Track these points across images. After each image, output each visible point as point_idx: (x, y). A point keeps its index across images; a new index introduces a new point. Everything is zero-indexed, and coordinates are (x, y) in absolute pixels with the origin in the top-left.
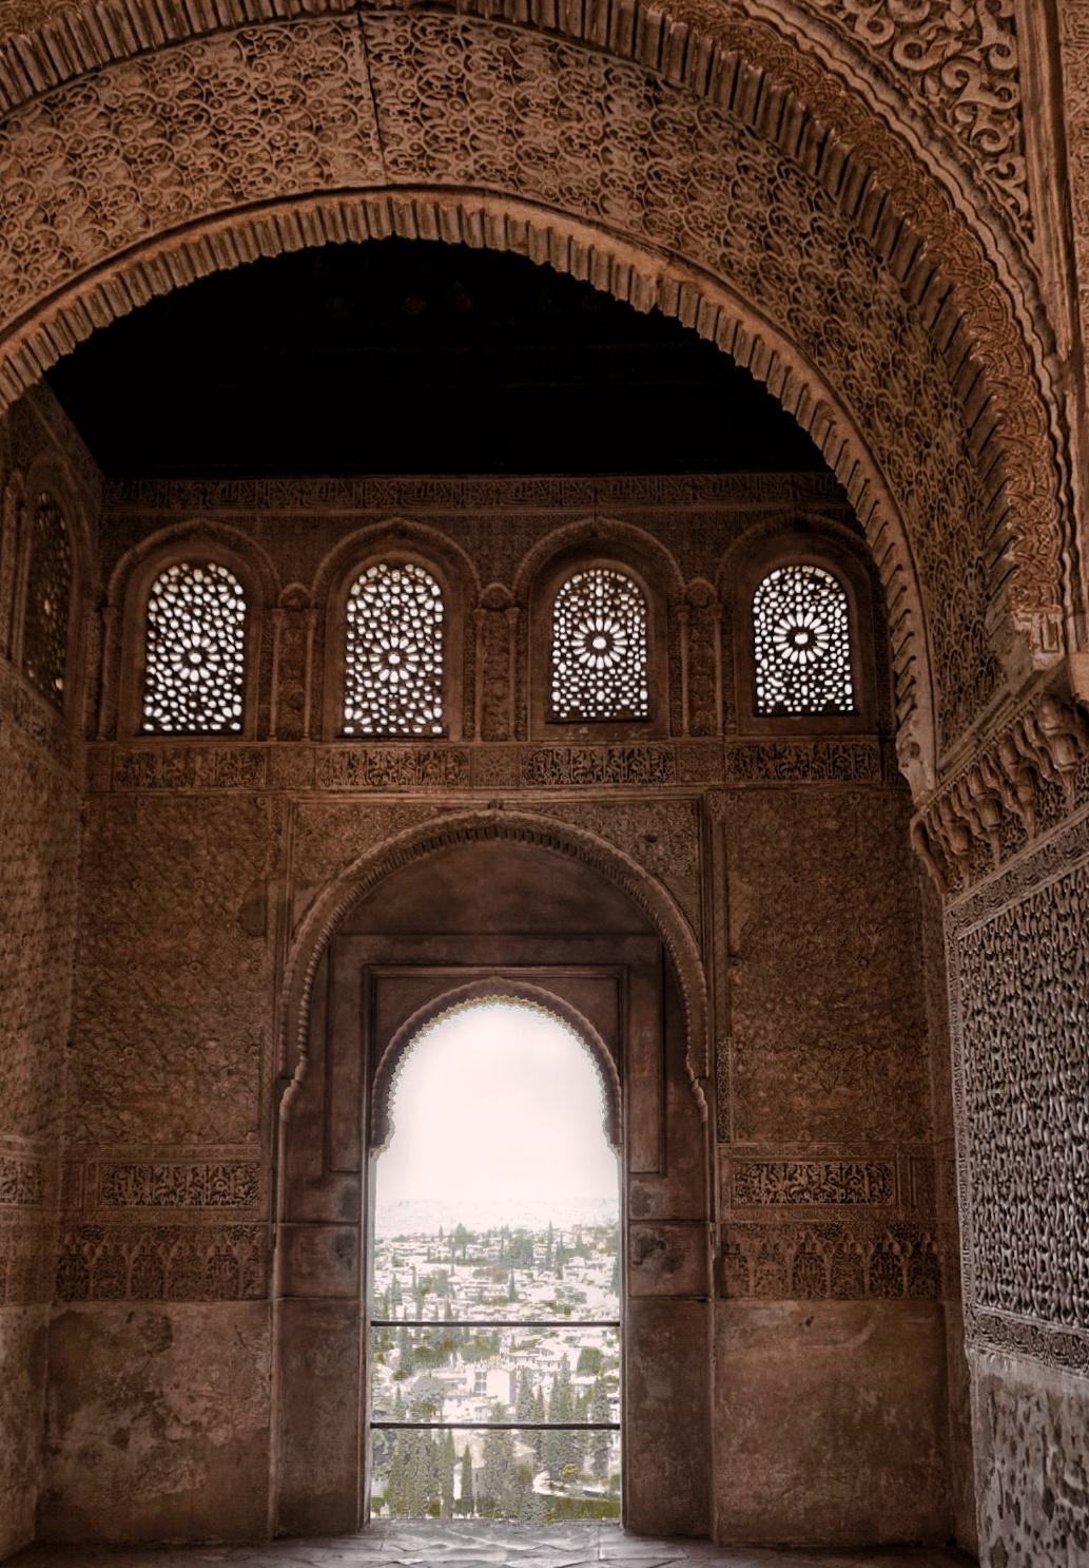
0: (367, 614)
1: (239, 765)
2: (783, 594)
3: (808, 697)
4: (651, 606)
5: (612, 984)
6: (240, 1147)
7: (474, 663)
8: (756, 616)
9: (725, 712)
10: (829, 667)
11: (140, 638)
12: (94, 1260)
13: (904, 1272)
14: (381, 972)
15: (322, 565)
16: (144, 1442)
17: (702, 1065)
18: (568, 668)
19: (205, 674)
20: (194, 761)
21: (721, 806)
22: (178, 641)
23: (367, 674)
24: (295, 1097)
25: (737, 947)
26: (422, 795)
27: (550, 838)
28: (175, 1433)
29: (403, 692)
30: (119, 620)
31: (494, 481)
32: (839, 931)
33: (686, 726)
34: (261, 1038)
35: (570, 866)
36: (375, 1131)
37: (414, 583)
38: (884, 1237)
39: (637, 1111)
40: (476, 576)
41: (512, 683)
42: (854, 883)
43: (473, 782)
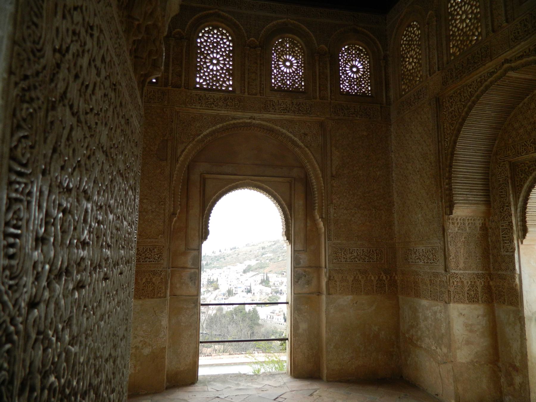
2: (349, 54)
3: (356, 89)
6: (156, 240)
9: (331, 93)
10: (363, 80)
14: (207, 176)
18: (277, 71)
25: (334, 173)
26: (226, 112)
27: (271, 131)
34: (165, 199)
36: (204, 234)
37: (222, 34)
38: (381, 274)
40: (246, 35)
41: (259, 74)
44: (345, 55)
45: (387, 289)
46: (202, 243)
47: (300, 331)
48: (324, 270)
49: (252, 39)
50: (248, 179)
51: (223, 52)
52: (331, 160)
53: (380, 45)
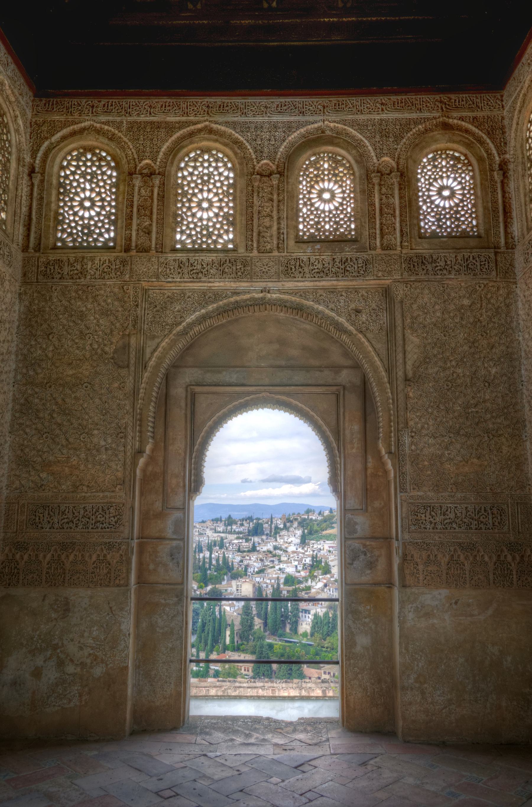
0: (189, 179)
1: (113, 267)
2: (435, 167)
3: (450, 227)
4: (357, 174)
5: (334, 397)
6: (113, 494)
7: (252, 207)
8: (418, 180)
9: (402, 235)
10: (463, 210)
11: (54, 193)
12: (23, 562)
13: (514, 573)
14: (198, 389)
15: (163, 150)
16: (51, 675)
17: (390, 445)
18: (308, 210)
19: (93, 213)
20: (86, 264)
21: (400, 292)
22: (77, 194)
23: (189, 214)
24: (147, 464)
25: (410, 374)
26: (221, 284)
27: (298, 309)
28: (70, 669)
29: (211, 224)
30: (42, 181)
31: (264, 101)
32: (471, 366)
33: (378, 244)
34: (125, 428)
35: (308, 327)
36: (196, 484)
37: (217, 160)
38: (502, 551)
39: (349, 473)
40: (254, 157)
41: (275, 218)
42: (480, 337)
43: (251, 276)
44: (429, 170)
45: (515, 579)
46: (191, 498)
47: (358, 649)
48: (395, 544)
49: (265, 161)
50: (265, 391)
51: (217, 188)
52: (405, 354)
53: (491, 145)
